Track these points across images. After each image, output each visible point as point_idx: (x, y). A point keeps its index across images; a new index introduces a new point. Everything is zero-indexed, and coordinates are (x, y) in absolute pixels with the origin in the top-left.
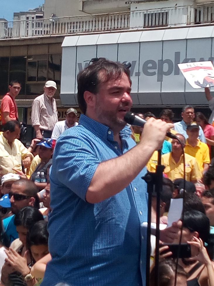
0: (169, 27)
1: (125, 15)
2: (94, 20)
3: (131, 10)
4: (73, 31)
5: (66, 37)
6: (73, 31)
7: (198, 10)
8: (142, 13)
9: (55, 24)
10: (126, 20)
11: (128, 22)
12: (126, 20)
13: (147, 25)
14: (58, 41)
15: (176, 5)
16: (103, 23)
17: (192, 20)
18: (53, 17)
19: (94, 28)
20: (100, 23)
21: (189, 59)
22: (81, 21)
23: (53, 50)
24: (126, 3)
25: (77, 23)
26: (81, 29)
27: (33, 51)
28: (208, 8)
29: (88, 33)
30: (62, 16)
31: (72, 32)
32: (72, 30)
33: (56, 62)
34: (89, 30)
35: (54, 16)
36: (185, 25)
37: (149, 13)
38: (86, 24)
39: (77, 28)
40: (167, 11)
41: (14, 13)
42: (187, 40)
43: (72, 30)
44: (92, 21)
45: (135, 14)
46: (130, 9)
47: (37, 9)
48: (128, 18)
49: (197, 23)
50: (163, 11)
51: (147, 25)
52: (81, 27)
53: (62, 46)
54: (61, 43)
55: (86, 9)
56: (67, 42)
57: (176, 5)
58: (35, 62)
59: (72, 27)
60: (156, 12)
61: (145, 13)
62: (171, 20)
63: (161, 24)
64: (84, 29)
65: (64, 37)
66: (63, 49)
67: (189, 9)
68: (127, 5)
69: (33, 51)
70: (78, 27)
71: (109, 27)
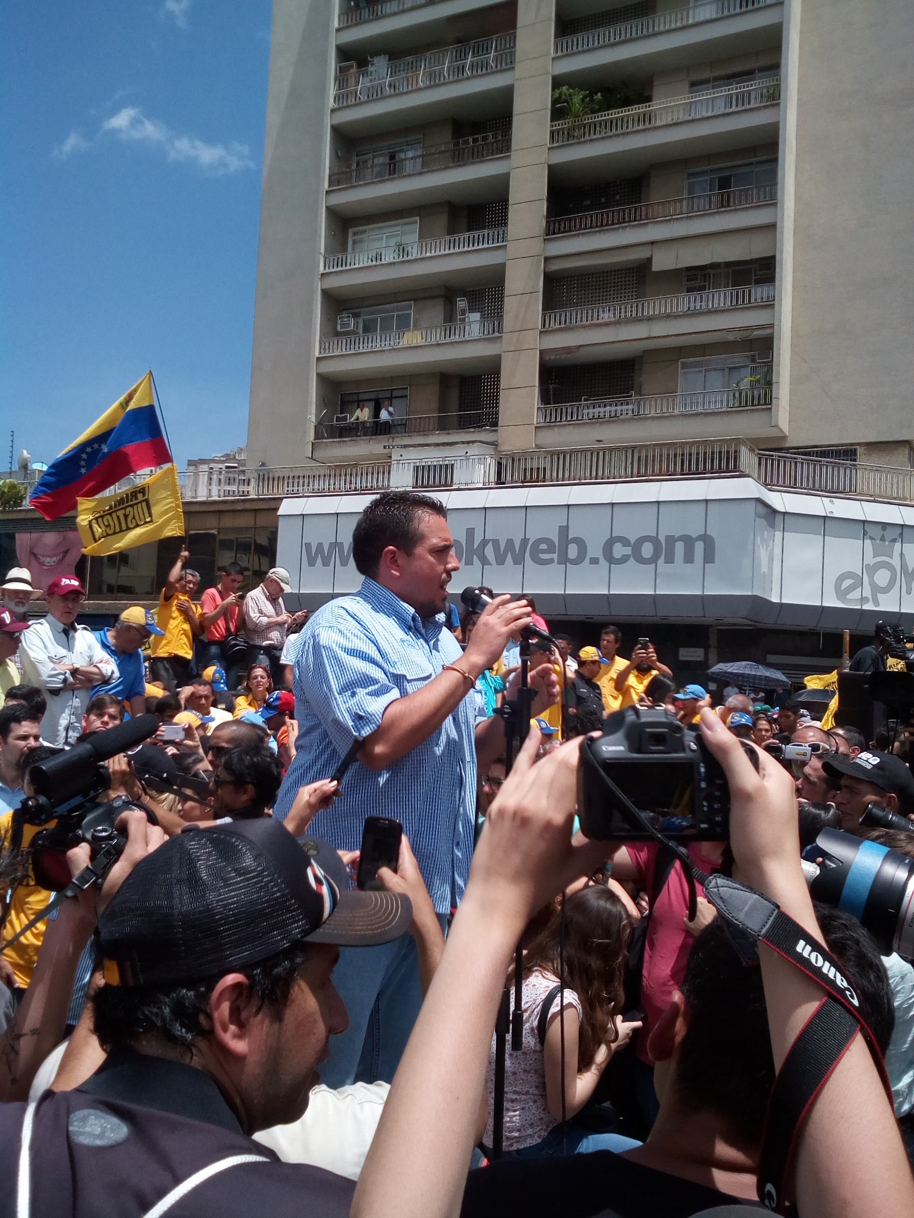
0: (455, 487)
1: (384, 466)
2: (332, 473)
3: (393, 459)
4: (298, 490)
5: (285, 500)
6: (298, 490)
7: (504, 462)
8: (412, 465)
9: (264, 477)
10: (386, 475)
11: (389, 478)
12: (386, 475)
13: (420, 483)
14: (272, 505)
15: (467, 453)
16: (343, 478)
17: (493, 477)
18: (261, 466)
19: (332, 487)
20: (343, 478)
21: (490, 540)
22: (312, 474)
23: (262, 520)
24: (385, 447)
25: (304, 477)
26: (311, 487)
27: (228, 522)
28: (519, 460)
29: (320, 494)
30: (277, 466)
31: (295, 491)
32: (296, 488)
33: (263, 540)
34: (324, 489)
35: (263, 465)
36: (481, 486)
37: (424, 464)
38: (319, 480)
39: (298, 486)
40: (453, 462)
41: (189, 461)
42: (485, 509)
43: (296, 488)
44: (330, 476)
45: (401, 465)
46: (390, 457)
47: (227, 455)
48: (389, 473)
49: (500, 482)
50: (447, 462)
51: (420, 483)
52: (311, 484)
53: (280, 513)
54: (277, 509)
55: (318, 455)
56: (287, 507)
57: (467, 453)
58: (231, 541)
59: (296, 484)
60: (435, 463)
61: (418, 464)
62: (459, 477)
63: (443, 482)
64: (316, 487)
65: (281, 499)
66: (280, 518)
67: (489, 460)
68: (386, 451)
69: (228, 522)
70: (306, 483)
71: (358, 486)
